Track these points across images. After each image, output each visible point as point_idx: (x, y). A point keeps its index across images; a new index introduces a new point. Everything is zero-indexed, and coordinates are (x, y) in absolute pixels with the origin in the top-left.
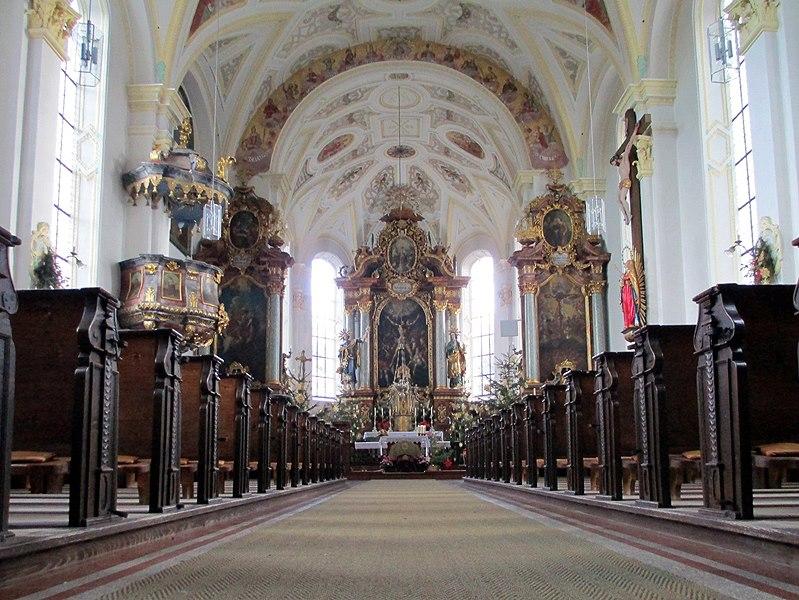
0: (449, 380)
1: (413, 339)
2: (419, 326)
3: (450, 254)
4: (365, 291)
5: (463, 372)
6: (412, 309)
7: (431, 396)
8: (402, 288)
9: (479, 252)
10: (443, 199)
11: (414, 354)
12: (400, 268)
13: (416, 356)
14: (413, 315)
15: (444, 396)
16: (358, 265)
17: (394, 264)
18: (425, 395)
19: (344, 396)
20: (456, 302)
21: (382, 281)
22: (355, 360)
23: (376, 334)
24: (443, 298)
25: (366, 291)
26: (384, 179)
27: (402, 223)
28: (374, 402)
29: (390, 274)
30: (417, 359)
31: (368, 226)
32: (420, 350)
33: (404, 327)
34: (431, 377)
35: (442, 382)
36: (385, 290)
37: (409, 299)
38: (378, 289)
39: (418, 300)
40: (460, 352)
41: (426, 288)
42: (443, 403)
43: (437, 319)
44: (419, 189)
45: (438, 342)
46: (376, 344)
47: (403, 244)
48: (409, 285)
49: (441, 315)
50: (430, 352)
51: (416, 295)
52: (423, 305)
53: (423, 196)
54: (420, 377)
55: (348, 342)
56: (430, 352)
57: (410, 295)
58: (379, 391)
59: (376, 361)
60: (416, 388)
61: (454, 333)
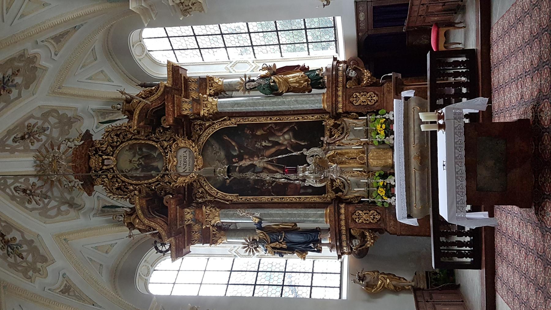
0: (314, 91)
1: (258, 145)
2: (239, 134)
3: (134, 91)
4: (189, 216)
5: (304, 69)
6: (216, 146)
7: (337, 116)
8: (184, 161)
9: (135, 52)
10: (54, 103)
11: (277, 144)
12: (159, 165)
13: (281, 140)
14: (227, 147)
15: (337, 96)
16: (150, 228)
17: (153, 173)
18: (336, 126)
19: (340, 248)
20: (204, 82)
21: (177, 191)
22: (287, 231)
23: (251, 199)
24: (197, 101)
25: (189, 214)
26: (24, 191)
27: (93, 162)
28: (349, 203)
29: (167, 179)
30: (285, 139)
31: (107, 209)
32: (273, 135)
33: (241, 158)
34: (310, 118)
35: (317, 100)
36: (190, 186)
37: (203, 152)
38: (188, 196)
39: (203, 139)
40: (274, 74)
41: (186, 126)
42: (348, 96)
43: (229, 109)
44: (43, 137)
45: (260, 108)
46: (265, 199)
47: (126, 161)
48: (181, 152)
49: (222, 104)
50: (275, 119)
51: (196, 141)
52: (211, 131)
53: (55, 133)
54: (310, 132)
55: (261, 241)
56: (275, 119)
57: (195, 149)
58: (330, 195)
59: (288, 199)
60: (325, 139)
61: (248, 85)
